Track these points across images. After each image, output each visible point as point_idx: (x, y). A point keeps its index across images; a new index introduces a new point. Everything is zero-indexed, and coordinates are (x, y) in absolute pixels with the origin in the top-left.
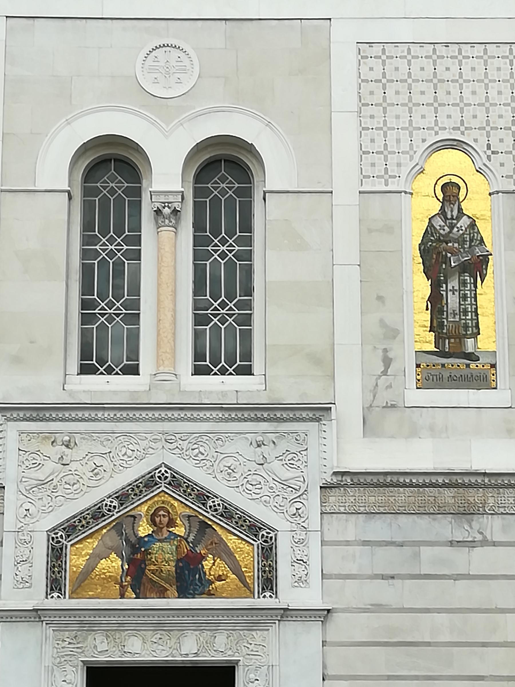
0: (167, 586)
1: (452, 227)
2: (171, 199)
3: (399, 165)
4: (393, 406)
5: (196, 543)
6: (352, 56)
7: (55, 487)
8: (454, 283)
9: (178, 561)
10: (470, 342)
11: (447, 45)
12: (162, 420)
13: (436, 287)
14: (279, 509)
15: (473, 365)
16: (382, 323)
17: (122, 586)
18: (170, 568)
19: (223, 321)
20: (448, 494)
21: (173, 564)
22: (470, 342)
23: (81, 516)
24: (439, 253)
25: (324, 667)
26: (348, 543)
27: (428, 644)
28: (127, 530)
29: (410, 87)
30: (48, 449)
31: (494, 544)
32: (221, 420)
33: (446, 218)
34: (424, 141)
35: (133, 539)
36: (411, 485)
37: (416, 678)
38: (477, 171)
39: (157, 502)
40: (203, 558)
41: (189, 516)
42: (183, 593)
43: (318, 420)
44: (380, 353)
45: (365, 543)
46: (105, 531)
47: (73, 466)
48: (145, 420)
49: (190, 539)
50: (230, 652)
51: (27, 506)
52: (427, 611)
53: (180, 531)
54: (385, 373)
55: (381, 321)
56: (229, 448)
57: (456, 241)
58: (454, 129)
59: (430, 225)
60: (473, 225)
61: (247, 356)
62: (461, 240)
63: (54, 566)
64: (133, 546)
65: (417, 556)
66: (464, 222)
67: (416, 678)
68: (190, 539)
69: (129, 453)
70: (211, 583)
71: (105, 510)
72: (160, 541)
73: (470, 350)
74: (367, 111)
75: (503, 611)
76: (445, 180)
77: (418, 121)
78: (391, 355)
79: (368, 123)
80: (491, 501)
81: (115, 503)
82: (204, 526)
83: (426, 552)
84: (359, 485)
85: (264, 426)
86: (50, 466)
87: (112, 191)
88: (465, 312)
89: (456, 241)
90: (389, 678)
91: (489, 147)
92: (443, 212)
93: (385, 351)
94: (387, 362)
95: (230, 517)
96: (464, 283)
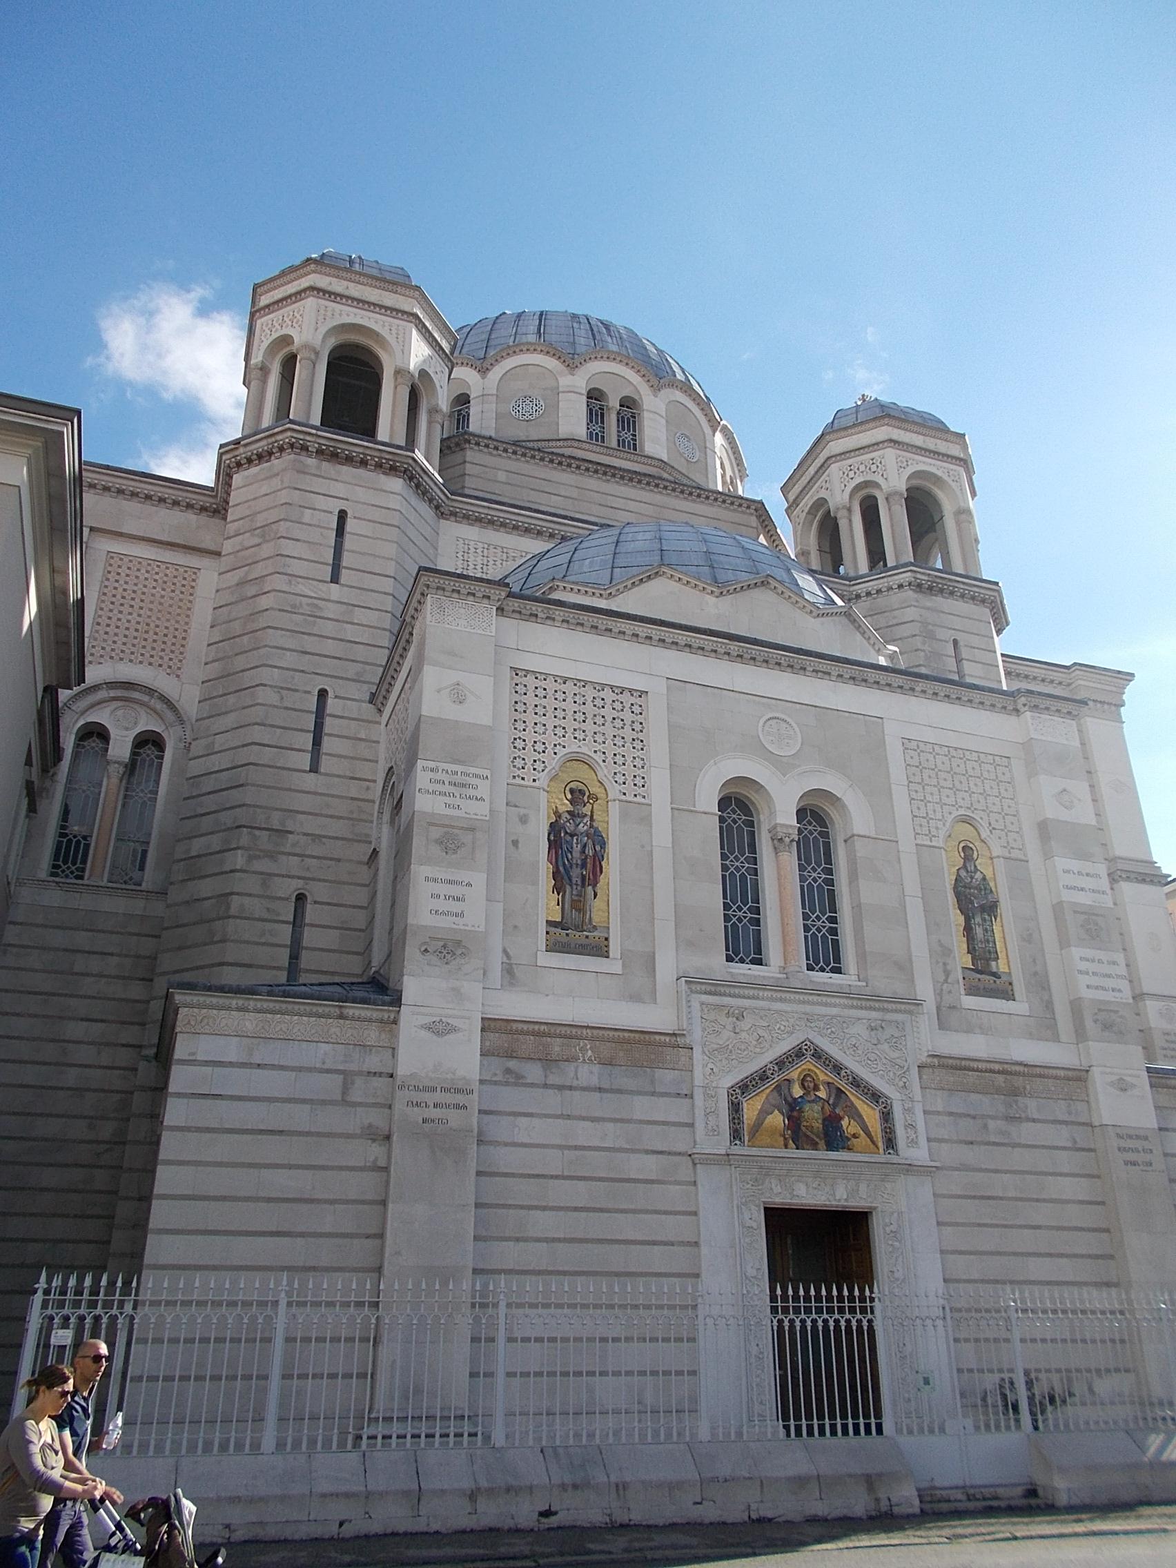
0: (817, 1140)
2: (791, 832)
3: (937, 828)
4: (954, 1007)
5: (835, 1105)
7: (731, 1052)
8: (978, 919)
9: (824, 1120)
10: (993, 963)
11: (956, 749)
12: (804, 1002)
13: (968, 920)
14: (891, 1082)
15: (998, 981)
16: (941, 945)
17: (785, 1139)
18: (818, 1125)
19: (819, 930)
20: (1000, 1079)
21: (820, 1121)
22: (993, 963)
23: (751, 1078)
24: (966, 896)
26: (938, 1113)
27: (1001, 1198)
29: (937, 775)
30: (723, 1019)
31: (1034, 1121)
32: (846, 1006)
33: (967, 872)
34: (950, 813)
35: (789, 1099)
36: (977, 1070)
37: (997, 1226)
38: (983, 841)
39: (804, 1070)
40: (841, 1118)
41: (829, 1083)
42: (830, 1147)
43: (910, 1013)
45: (951, 1114)
46: (768, 1091)
47: (744, 1035)
48: (794, 1001)
49: (831, 1102)
50: (869, 1200)
51: (711, 1066)
52: (996, 1171)
53: (822, 1094)
54: (946, 981)
55: (939, 941)
56: (854, 1030)
57: (975, 888)
58: (968, 808)
59: (958, 875)
60: (984, 879)
61: (837, 959)
63: (734, 1118)
64: (790, 1105)
65: (985, 1126)
67: (997, 1226)
68: (831, 1102)
69: (782, 1028)
70: (849, 1139)
71: (769, 1073)
72: (809, 1102)
73: (994, 970)
76: (962, 845)
77: (945, 800)
78: (949, 967)
79: (914, 795)
80: (1028, 1087)
81: (776, 1069)
82: (839, 1091)
83: (992, 1124)
84: (941, 1066)
85: (874, 1014)
86: (727, 1034)
87: (735, 821)
89: (975, 888)
90: (979, 1225)
91: (990, 824)
92: (965, 867)
93: (945, 964)
94: (947, 973)
95: (858, 1086)
96: (984, 920)
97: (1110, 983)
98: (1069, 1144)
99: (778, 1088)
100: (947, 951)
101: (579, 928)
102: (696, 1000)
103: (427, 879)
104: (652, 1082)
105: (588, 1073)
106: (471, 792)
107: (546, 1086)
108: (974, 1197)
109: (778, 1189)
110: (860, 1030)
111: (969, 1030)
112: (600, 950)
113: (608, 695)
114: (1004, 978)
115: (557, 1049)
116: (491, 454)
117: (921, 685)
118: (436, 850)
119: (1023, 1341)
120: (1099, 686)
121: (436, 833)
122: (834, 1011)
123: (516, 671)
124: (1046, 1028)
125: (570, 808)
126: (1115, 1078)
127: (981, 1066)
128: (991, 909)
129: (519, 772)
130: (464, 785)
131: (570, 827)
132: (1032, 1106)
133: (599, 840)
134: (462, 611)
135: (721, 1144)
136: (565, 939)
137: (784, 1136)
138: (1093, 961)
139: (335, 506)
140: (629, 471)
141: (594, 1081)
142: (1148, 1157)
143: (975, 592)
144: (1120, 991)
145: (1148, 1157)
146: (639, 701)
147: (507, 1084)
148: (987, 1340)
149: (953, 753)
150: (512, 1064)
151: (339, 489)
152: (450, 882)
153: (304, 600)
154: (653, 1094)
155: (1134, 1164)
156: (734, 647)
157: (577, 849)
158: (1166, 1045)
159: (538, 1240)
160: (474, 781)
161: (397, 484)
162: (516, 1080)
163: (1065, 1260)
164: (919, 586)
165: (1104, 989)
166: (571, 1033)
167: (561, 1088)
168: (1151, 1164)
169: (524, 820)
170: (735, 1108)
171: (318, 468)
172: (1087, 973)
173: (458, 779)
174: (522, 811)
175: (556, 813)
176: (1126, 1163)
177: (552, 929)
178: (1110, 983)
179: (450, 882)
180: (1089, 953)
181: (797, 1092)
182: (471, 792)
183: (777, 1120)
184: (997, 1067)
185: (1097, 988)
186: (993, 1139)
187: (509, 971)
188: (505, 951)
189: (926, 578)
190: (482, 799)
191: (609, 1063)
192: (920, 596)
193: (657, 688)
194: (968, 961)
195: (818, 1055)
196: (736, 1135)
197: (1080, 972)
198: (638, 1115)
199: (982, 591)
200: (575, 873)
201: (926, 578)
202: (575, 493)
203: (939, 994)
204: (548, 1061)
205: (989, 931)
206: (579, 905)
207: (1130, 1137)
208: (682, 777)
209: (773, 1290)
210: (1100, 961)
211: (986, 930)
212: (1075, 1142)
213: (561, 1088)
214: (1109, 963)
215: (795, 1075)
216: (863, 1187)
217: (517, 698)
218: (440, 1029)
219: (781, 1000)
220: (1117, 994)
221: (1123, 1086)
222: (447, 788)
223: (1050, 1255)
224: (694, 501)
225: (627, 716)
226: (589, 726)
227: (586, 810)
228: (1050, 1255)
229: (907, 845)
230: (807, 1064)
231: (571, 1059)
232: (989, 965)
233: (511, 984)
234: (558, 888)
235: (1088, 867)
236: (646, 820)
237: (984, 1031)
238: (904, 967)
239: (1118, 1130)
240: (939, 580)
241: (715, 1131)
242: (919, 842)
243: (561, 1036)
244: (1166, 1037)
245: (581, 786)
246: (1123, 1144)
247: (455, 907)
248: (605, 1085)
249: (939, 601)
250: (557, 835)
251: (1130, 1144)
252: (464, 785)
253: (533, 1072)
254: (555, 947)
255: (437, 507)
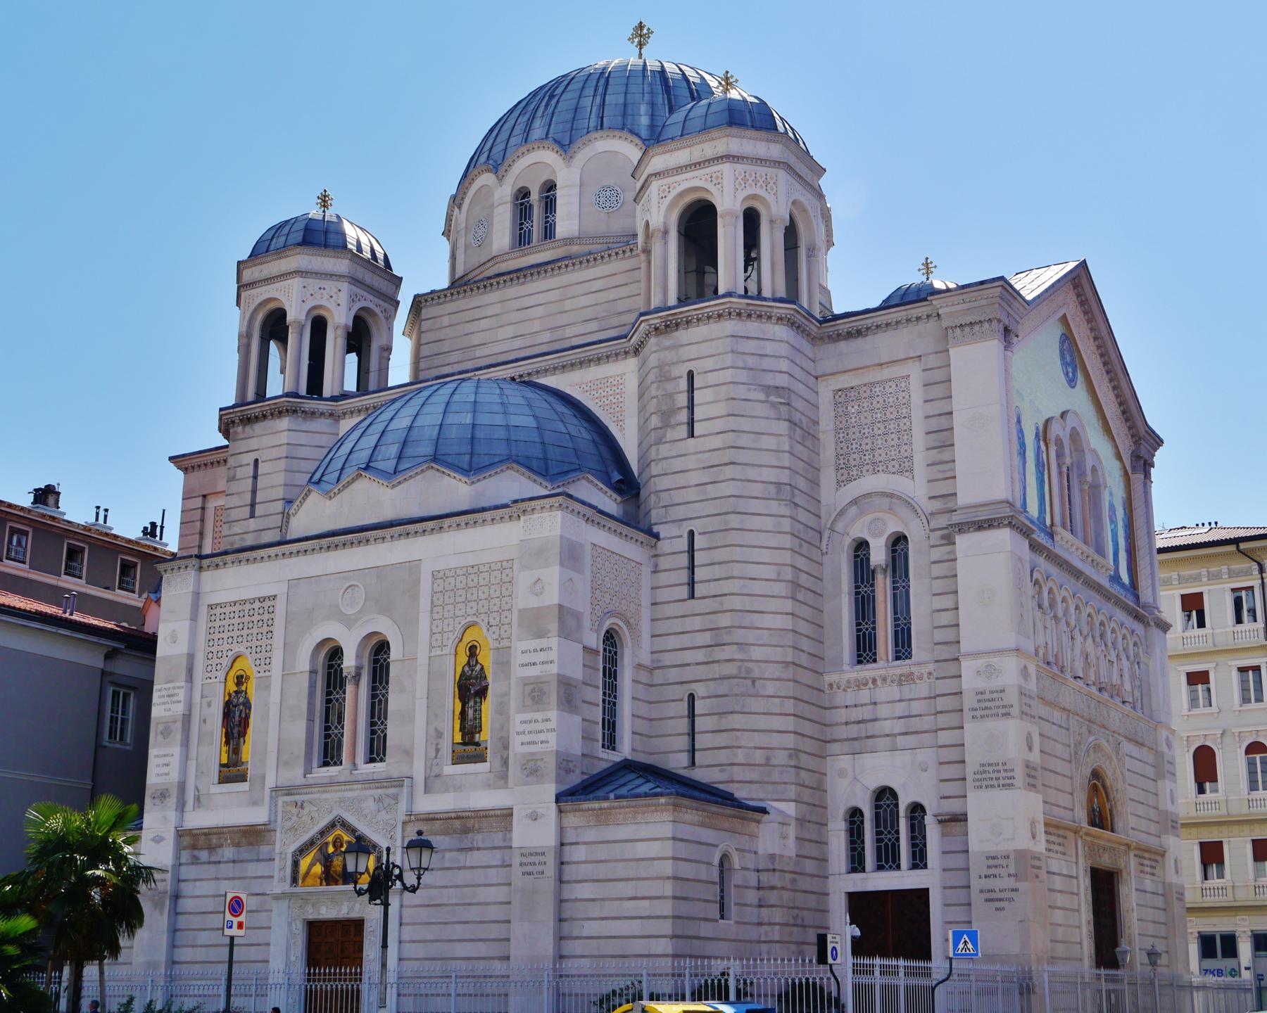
1: (472, 671)
6: (430, 578)
8: (471, 703)
10: (477, 736)
16: (436, 730)
20: (457, 824)
25: (401, 918)
28: (324, 850)
31: (478, 849)
32: (362, 789)
44: (434, 746)
52: (446, 887)
54: (436, 757)
59: (463, 671)
60: (482, 668)
62: (476, 678)
65: (444, 857)
66: (478, 667)
67: (440, 923)
73: (477, 739)
74: (436, 609)
75: (480, 886)
76: (476, 643)
79: (436, 616)
83: (448, 855)
86: (294, 818)
88: (475, 719)
92: (469, 662)
93: (437, 744)
94: (437, 751)
96: (475, 703)
97: (542, 737)
98: (499, 863)
99: (321, 849)
100: (439, 735)
101: (235, 765)
102: (282, 799)
103: (155, 757)
104: (258, 854)
105: (228, 852)
106: (176, 698)
107: (209, 863)
108: (428, 906)
109: (311, 911)
110: (370, 805)
111: (447, 790)
112: (242, 778)
113: (257, 605)
114: (483, 746)
115: (214, 841)
116: (439, 304)
117: (447, 522)
118: (160, 738)
119: (449, 995)
120: (965, 306)
121: (161, 727)
122: (356, 793)
123: (211, 607)
124: (502, 777)
125: (236, 689)
126: (529, 811)
127: (442, 816)
128: (482, 693)
129: (209, 675)
130: (173, 695)
131: (235, 700)
132: (479, 839)
133: (247, 705)
134: (179, 580)
135: (286, 887)
136: (228, 774)
137: (320, 878)
138: (530, 722)
139: (249, 458)
140: (532, 266)
141: (231, 857)
142: (540, 868)
143: (708, 313)
144: (547, 742)
145: (540, 868)
146: (272, 603)
147: (193, 864)
148: (421, 995)
149: (470, 570)
150: (196, 853)
151: (253, 444)
152: (165, 756)
153: (237, 537)
154: (258, 860)
155: (530, 874)
156: (324, 542)
157: (237, 714)
158: (978, 706)
159: (201, 946)
160: (176, 691)
161: (284, 423)
162: (195, 861)
163: (481, 943)
164: (656, 329)
165: (534, 743)
166: (219, 831)
167: (215, 863)
168: (543, 873)
169: (209, 705)
170: (296, 864)
171: (244, 432)
172: (524, 733)
173: (171, 692)
174: (209, 699)
175: (230, 695)
176: (524, 874)
177: (223, 769)
178: (542, 737)
179: (165, 756)
180: (528, 716)
181: (331, 849)
182: (176, 698)
183: (318, 869)
184: (453, 815)
185: (529, 743)
186: (447, 865)
187: (198, 799)
188: (197, 789)
189: (658, 321)
190: (180, 702)
191: (238, 845)
192: (661, 338)
193: (280, 589)
194: (458, 738)
195: (345, 825)
196: (294, 880)
197: (518, 733)
198: (250, 874)
199: (714, 309)
200: (235, 731)
201: (658, 321)
202: (497, 309)
203: (428, 767)
204: (211, 849)
205: (478, 711)
206: (235, 751)
207: (531, 854)
208: (290, 648)
209: (309, 970)
210: (537, 721)
211: (475, 711)
212: (504, 861)
213: (215, 863)
214: (543, 721)
215: (330, 839)
216: (357, 906)
217: (210, 624)
218: (158, 840)
219: (324, 792)
220: (544, 745)
221: (534, 817)
222: (166, 699)
223: (472, 940)
224: (594, 266)
225: (266, 617)
226: (245, 632)
227: (243, 688)
228: (472, 940)
229: (422, 660)
230: (339, 831)
231: (221, 846)
232: (473, 737)
233: (199, 807)
234: (227, 743)
235: (543, 643)
236: (268, 687)
237: (457, 789)
238: (408, 753)
239: (523, 851)
240: (670, 318)
241: (283, 880)
242: (432, 654)
243: (216, 834)
244: (981, 697)
245: (242, 673)
246: (525, 860)
247: (165, 770)
248: (236, 859)
249: (683, 335)
250: (229, 709)
251: (531, 859)
252: (173, 695)
253: (204, 855)
254: (224, 780)
255: (331, 415)
